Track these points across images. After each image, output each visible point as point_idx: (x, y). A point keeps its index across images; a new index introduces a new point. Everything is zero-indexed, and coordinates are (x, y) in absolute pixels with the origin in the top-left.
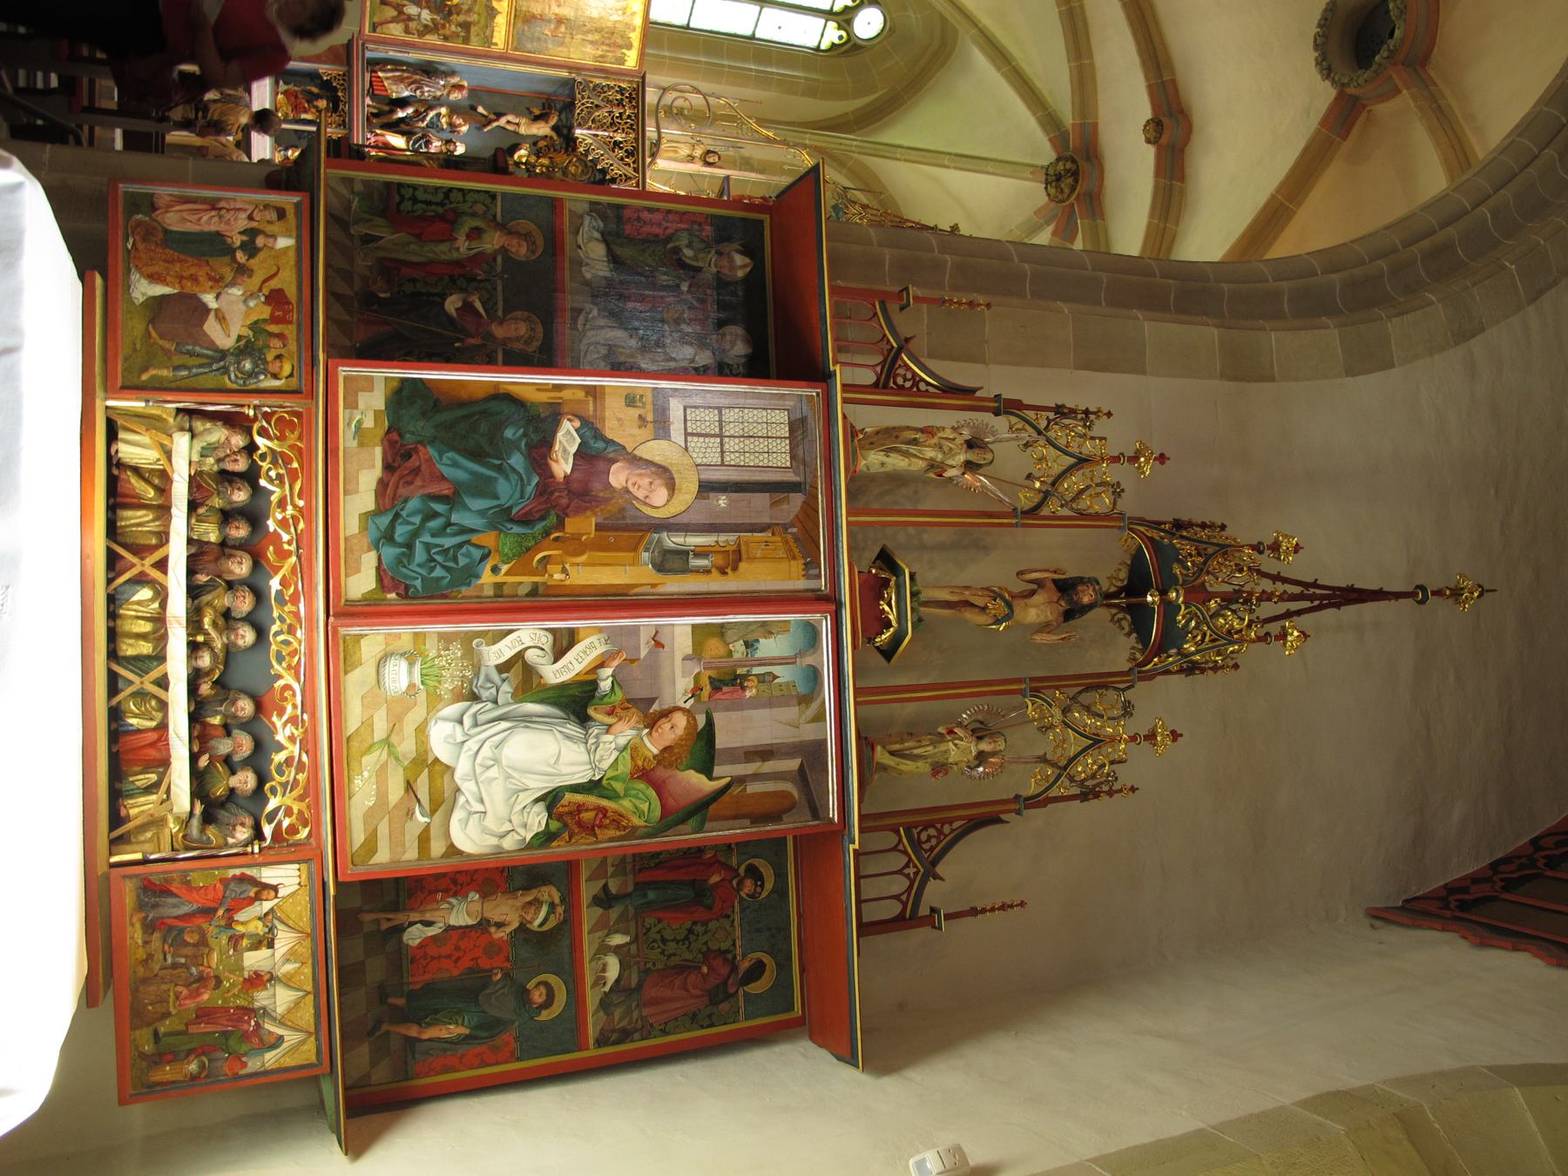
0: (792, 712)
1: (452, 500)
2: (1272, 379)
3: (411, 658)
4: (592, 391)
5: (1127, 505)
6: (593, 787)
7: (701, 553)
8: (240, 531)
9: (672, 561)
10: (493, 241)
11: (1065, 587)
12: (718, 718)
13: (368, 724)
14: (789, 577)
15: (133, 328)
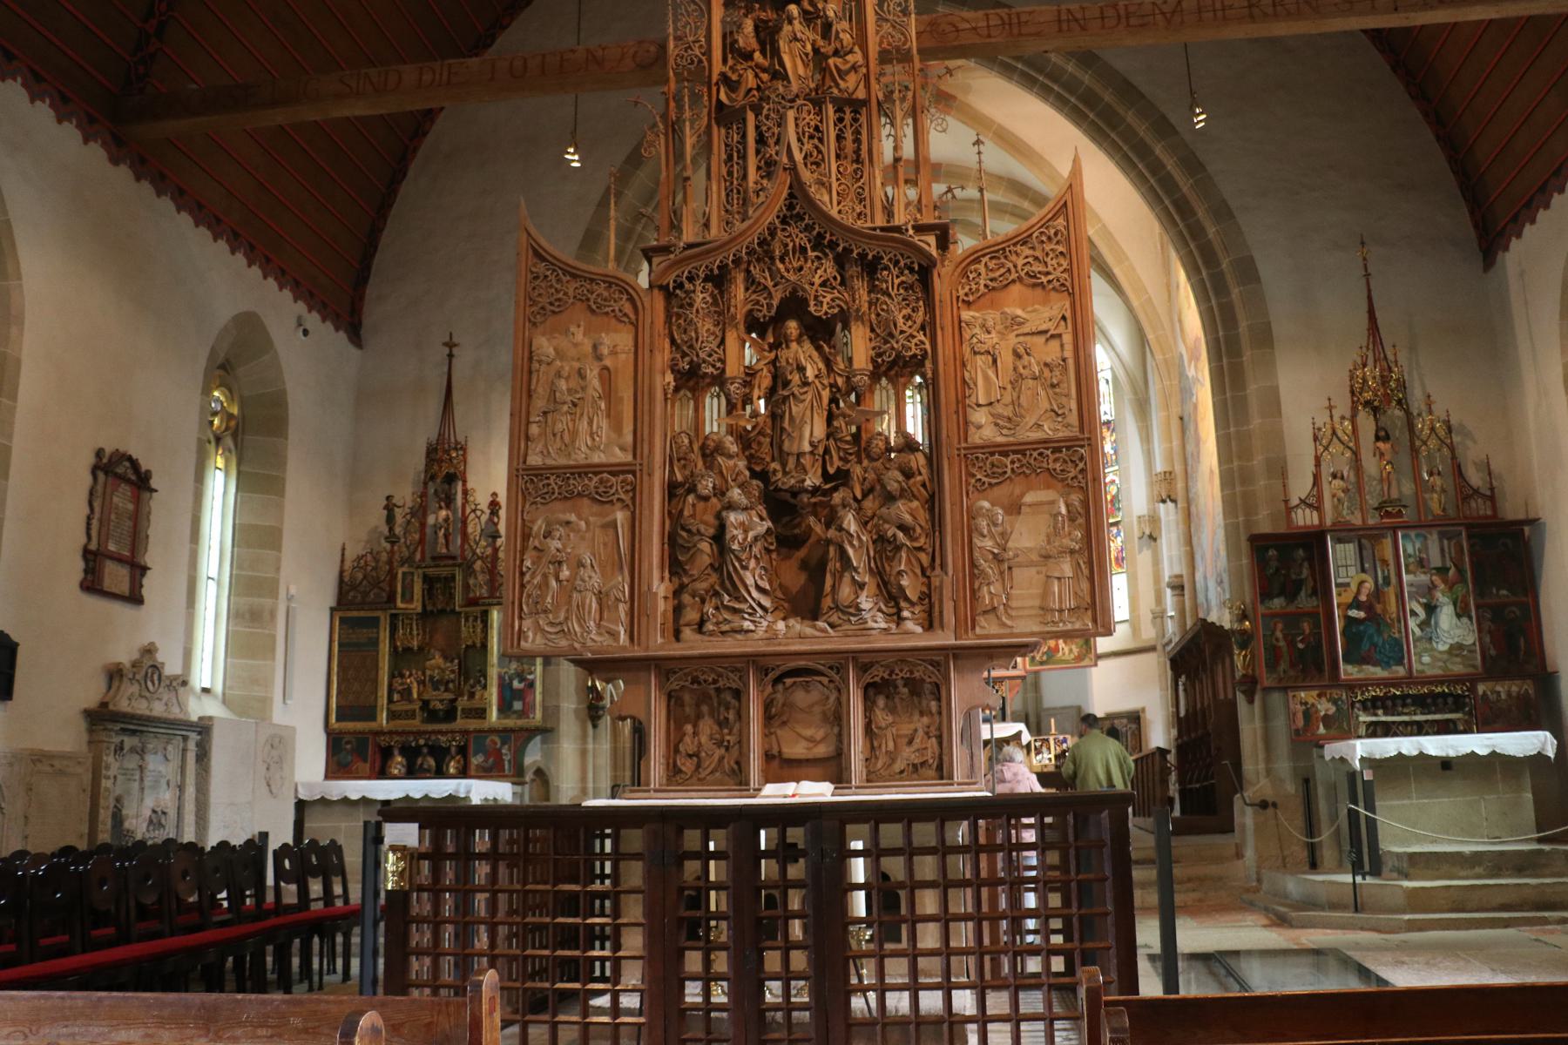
0: (1429, 542)
1: (1375, 645)
2: (1269, 323)
3: (1421, 656)
4: (1338, 607)
5: (1348, 414)
6: (1455, 605)
7: (1383, 572)
8: (1379, 703)
9: (1387, 581)
10: (1279, 634)
11: (1378, 438)
12: (1432, 566)
13: (1440, 667)
14: (1388, 543)
15: (1333, 732)
